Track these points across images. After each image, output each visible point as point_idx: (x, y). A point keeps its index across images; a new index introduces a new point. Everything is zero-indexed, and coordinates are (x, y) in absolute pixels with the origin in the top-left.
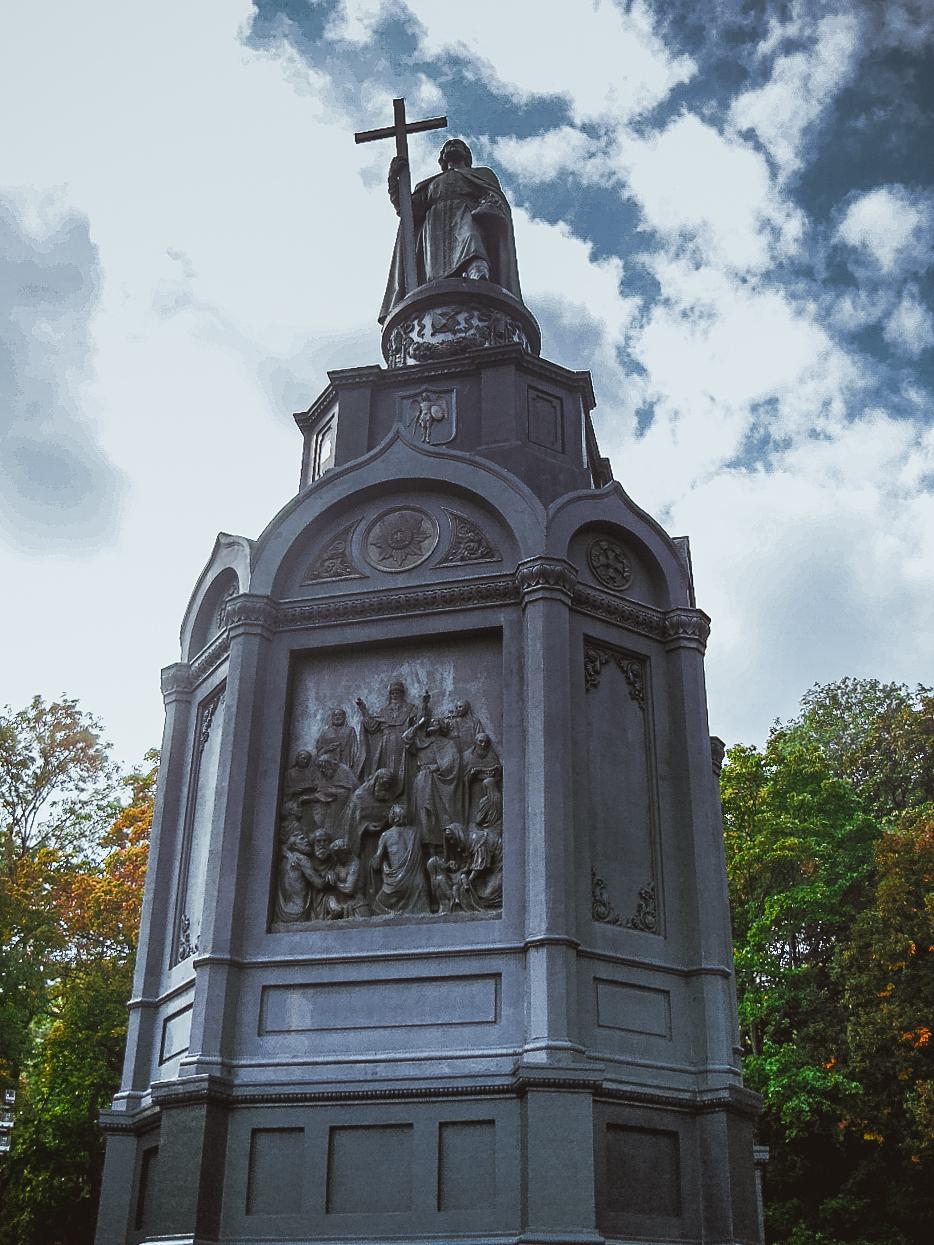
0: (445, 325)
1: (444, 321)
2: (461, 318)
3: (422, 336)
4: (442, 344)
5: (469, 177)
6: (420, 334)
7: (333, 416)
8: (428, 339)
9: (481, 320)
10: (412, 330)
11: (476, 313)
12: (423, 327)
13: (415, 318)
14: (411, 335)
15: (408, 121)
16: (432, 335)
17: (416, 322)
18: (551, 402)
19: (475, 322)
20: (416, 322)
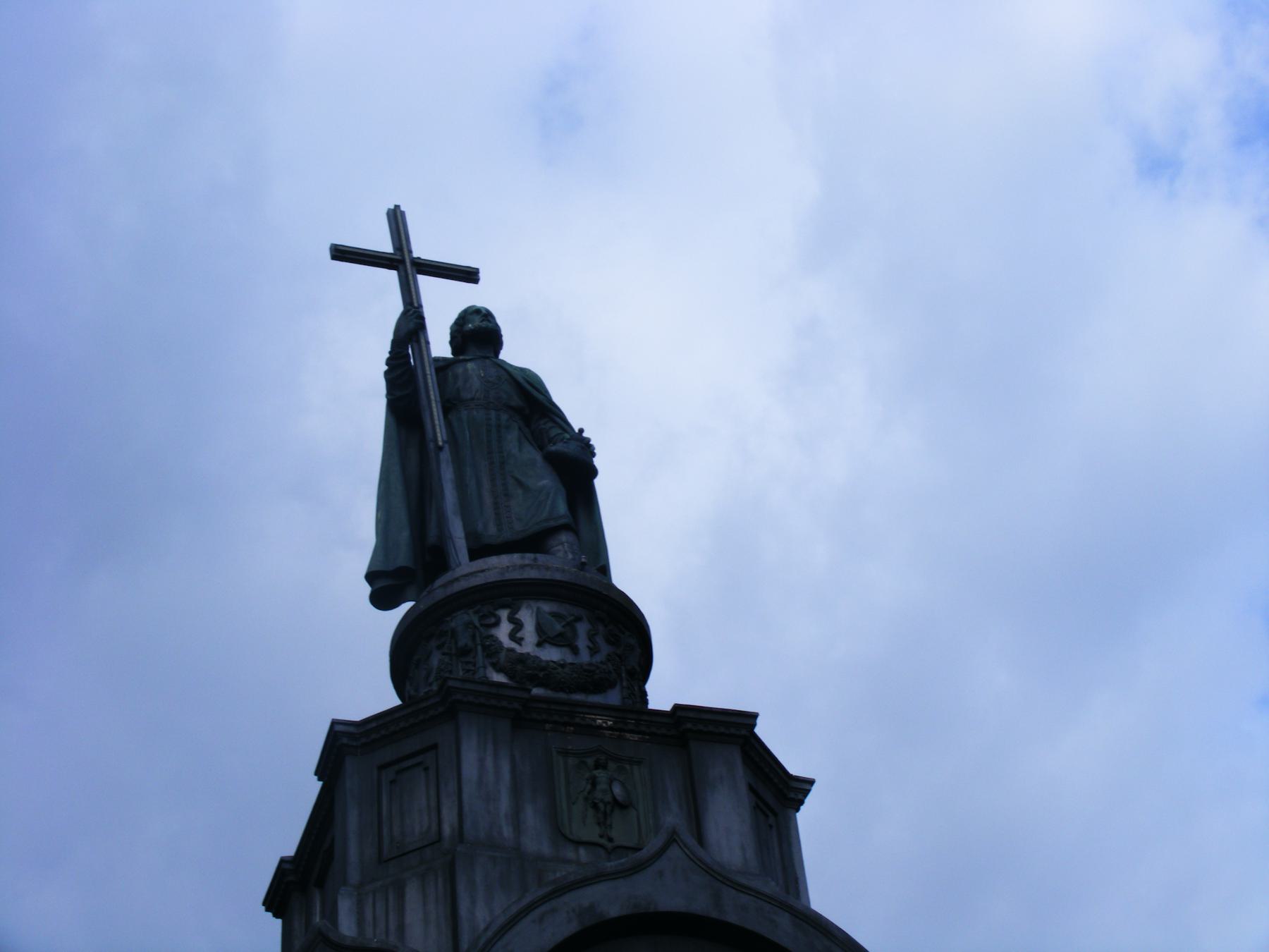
0: (561, 635)
1: (558, 627)
2: (582, 629)
3: (519, 641)
4: (563, 666)
5: (522, 381)
6: (512, 636)
7: (434, 747)
8: (529, 645)
9: (608, 641)
10: (497, 624)
11: (601, 628)
12: (518, 625)
13: (504, 607)
14: (494, 631)
15: (422, 249)
16: (539, 645)
17: (504, 614)
18: (767, 816)
19: (600, 640)
20: (504, 614)
